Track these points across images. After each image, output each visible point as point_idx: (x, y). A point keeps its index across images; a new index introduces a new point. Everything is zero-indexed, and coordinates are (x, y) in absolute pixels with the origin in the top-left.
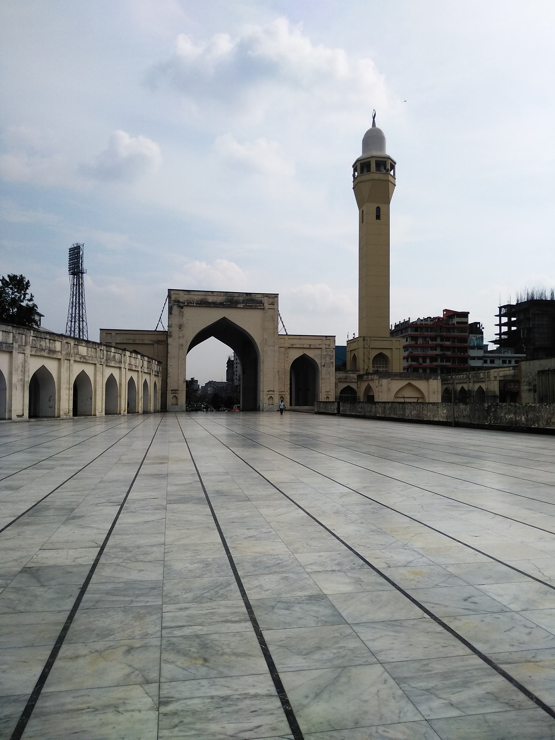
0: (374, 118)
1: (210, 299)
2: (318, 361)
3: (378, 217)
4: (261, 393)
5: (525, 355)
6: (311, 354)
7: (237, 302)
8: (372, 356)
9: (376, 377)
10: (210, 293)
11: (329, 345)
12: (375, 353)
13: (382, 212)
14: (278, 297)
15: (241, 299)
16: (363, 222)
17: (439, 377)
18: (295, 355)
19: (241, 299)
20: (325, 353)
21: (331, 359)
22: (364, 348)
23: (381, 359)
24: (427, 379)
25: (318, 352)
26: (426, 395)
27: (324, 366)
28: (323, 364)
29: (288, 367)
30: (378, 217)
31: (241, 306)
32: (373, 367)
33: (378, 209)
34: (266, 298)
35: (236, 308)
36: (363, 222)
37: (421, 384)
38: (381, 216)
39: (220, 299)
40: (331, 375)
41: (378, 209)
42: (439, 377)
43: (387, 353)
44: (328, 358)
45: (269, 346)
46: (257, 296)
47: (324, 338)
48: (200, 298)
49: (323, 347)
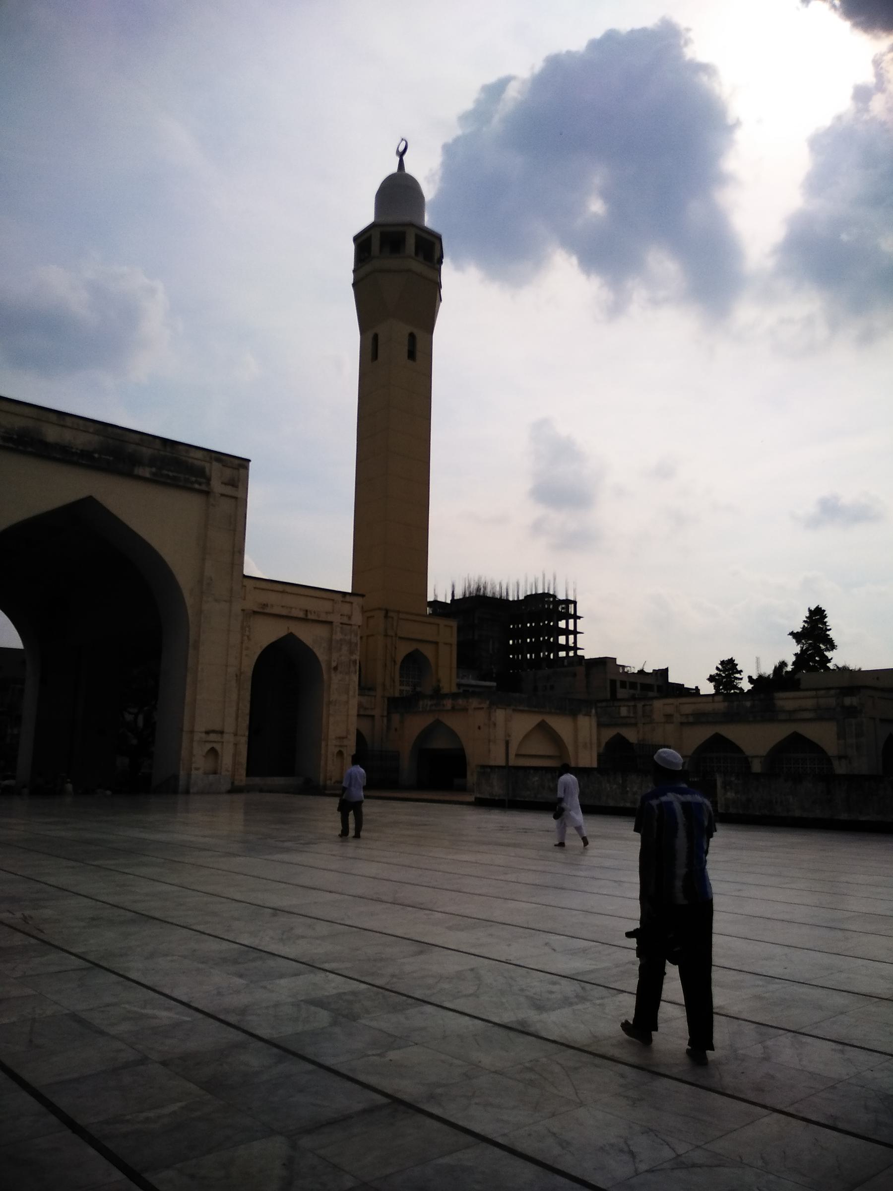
0: (401, 154)
1: (52, 434)
2: (321, 656)
3: (412, 355)
4: (185, 738)
5: (494, 684)
6: (307, 635)
7: (134, 460)
8: (399, 659)
9: (474, 703)
10: (53, 418)
11: (350, 618)
12: (403, 650)
13: (419, 346)
14: (246, 468)
15: (146, 452)
16: (375, 356)
17: (593, 711)
18: (267, 633)
19: (146, 452)
20: (338, 636)
21: (351, 652)
22: (386, 635)
23: (415, 663)
24: (574, 714)
25: (321, 631)
26: (570, 749)
27: (336, 668)
28: (334, 664)
29: (249, 665)
30: (412, 355)
31: (146, 472)
32: (401, 683)
33: (412, 336)
34: (216, 465)
35: (130, 475)
36: (375, 356)
37: (561, 725)
38: (419, 355)
39: (81, 440)
40: (351, 693)
41: (412, 336)
42: (593, 711)
43: (428, 651)
44: (345, 649)
45: (216, 600)
46: (193, 454)
47: (339, 598)
48: (19, 423)
49: (336, 619)
